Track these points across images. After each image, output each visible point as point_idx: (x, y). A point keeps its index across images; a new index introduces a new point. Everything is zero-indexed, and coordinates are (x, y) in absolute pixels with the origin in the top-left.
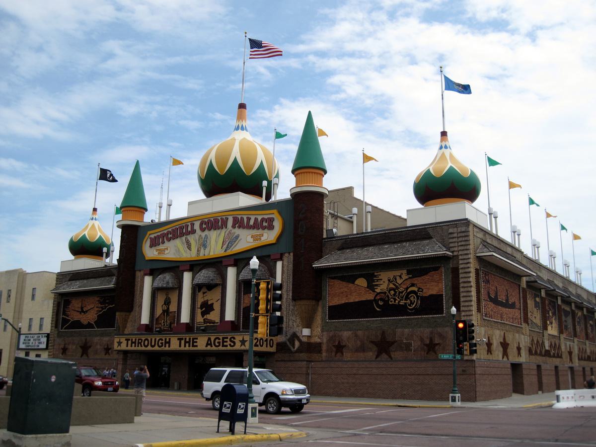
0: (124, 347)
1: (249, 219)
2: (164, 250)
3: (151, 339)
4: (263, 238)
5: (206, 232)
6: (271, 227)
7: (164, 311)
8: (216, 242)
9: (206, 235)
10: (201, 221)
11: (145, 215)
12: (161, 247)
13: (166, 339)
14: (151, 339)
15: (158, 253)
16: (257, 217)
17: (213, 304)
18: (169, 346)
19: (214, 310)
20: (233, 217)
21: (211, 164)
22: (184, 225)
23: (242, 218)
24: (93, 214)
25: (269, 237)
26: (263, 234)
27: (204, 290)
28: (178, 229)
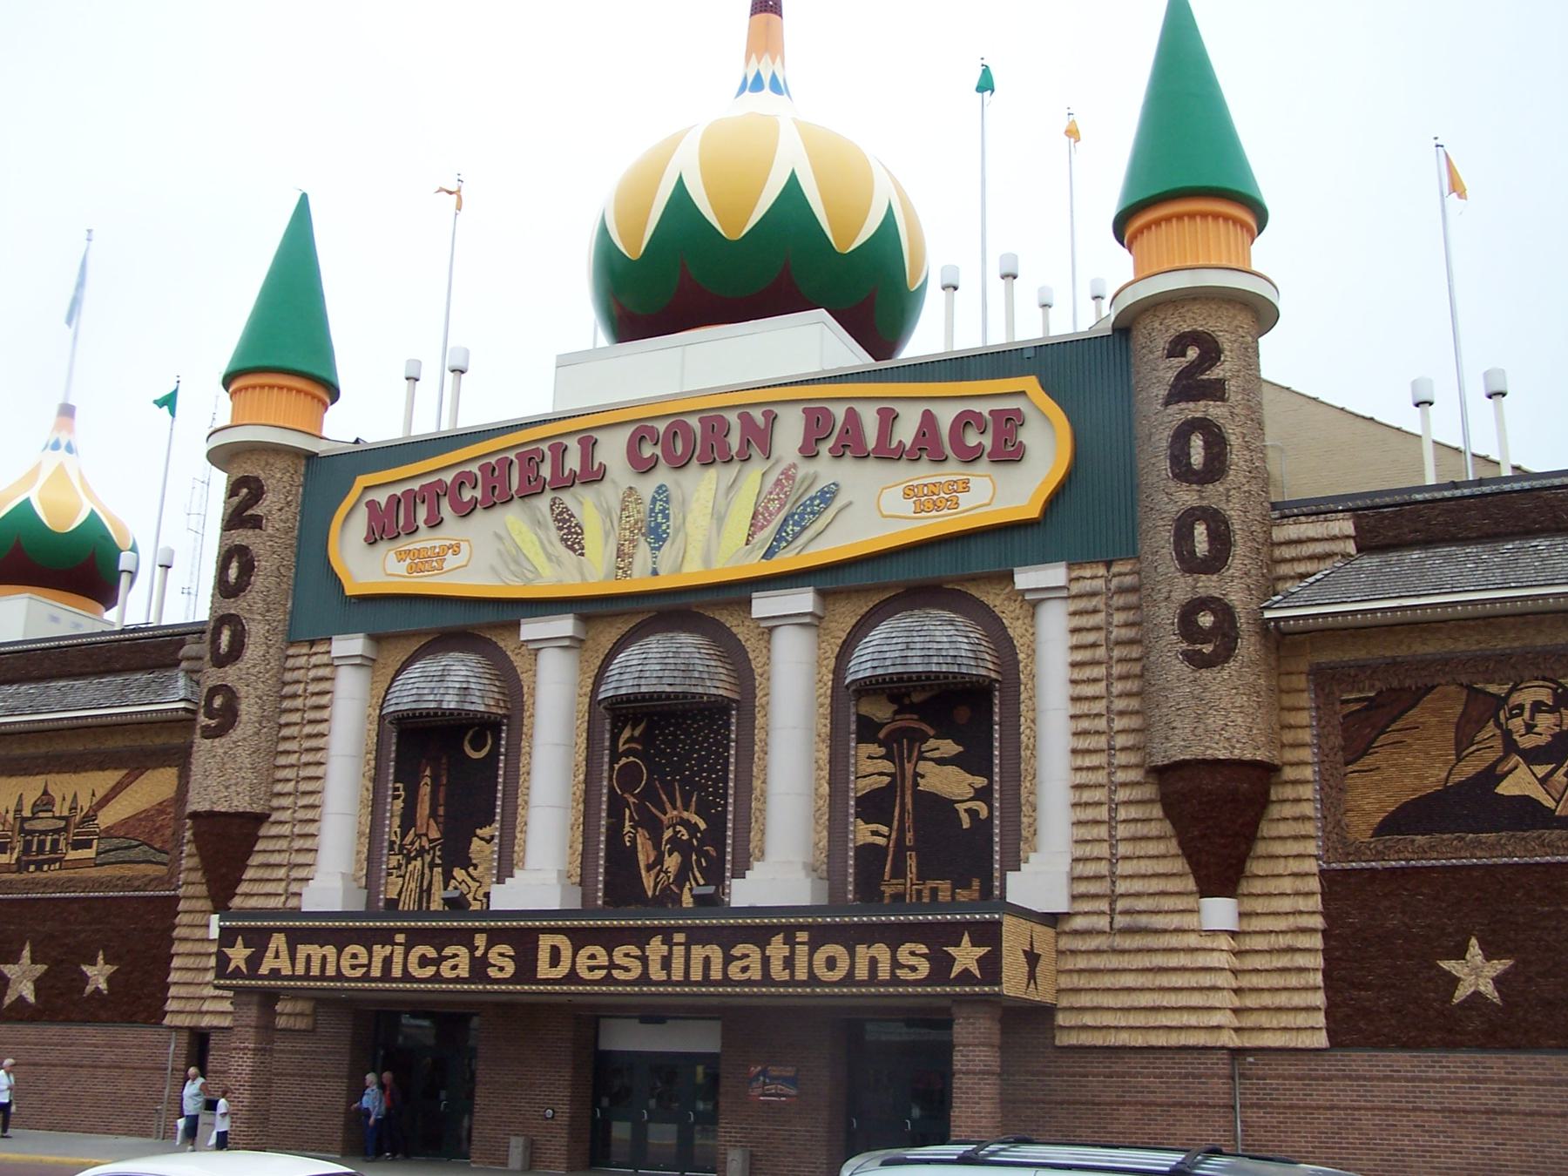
1: (888, 419)
2: (440, 556)
4: (965, 500)
5: (662, 476)
6: (1008, 453)
8: (719, 518)
9: (661, 489)
10: (632, 428)
11: (326, 415)
12: (425, 540)
15: (411, 570)
16: (935, 408)
20: (805, 411)
21: (680, 197)
22: (512, 455)
23: (852, 416)
24: (58, 427)
25: (1013, 493)
26: (966, 482)
28: (521, 468)
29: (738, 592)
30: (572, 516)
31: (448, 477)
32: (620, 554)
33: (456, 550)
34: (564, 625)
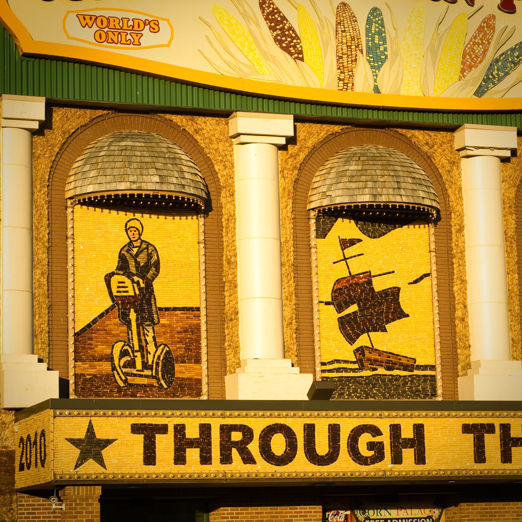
0: (124, 460)
3: (310, 430)
7: (121, 305)
13: (395, 429)
14: (310, 430)
17: (395, 292)
18: (420, 459)
19: (401, 315)
27: (345, 228)
29: (446, 121)
30: (284, 18)
32: (341, 68)
34: (283, 125)
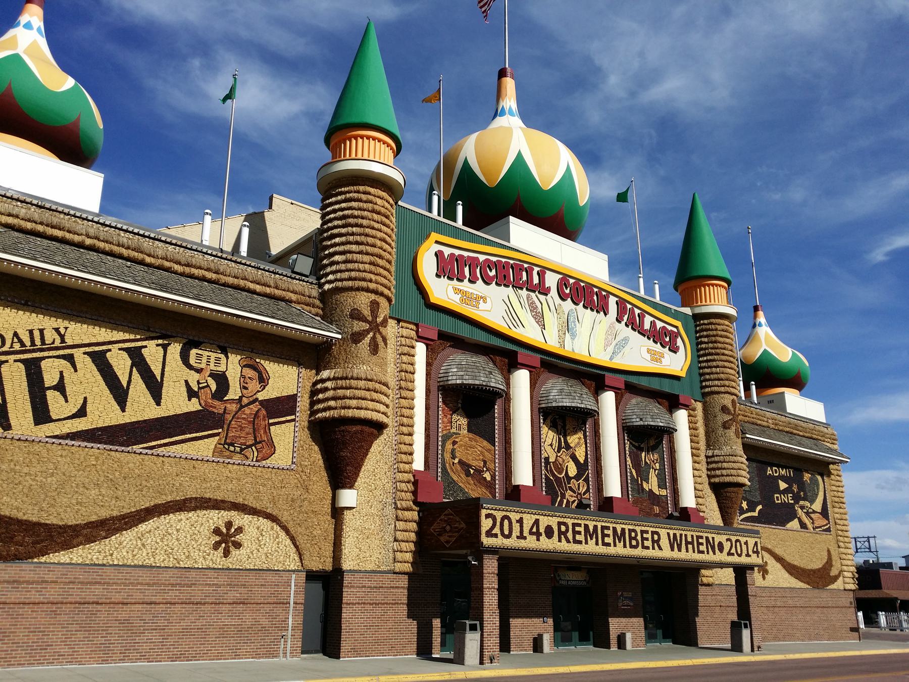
12: (465, 285)
31: (482, 258)
33: (485, 302)
